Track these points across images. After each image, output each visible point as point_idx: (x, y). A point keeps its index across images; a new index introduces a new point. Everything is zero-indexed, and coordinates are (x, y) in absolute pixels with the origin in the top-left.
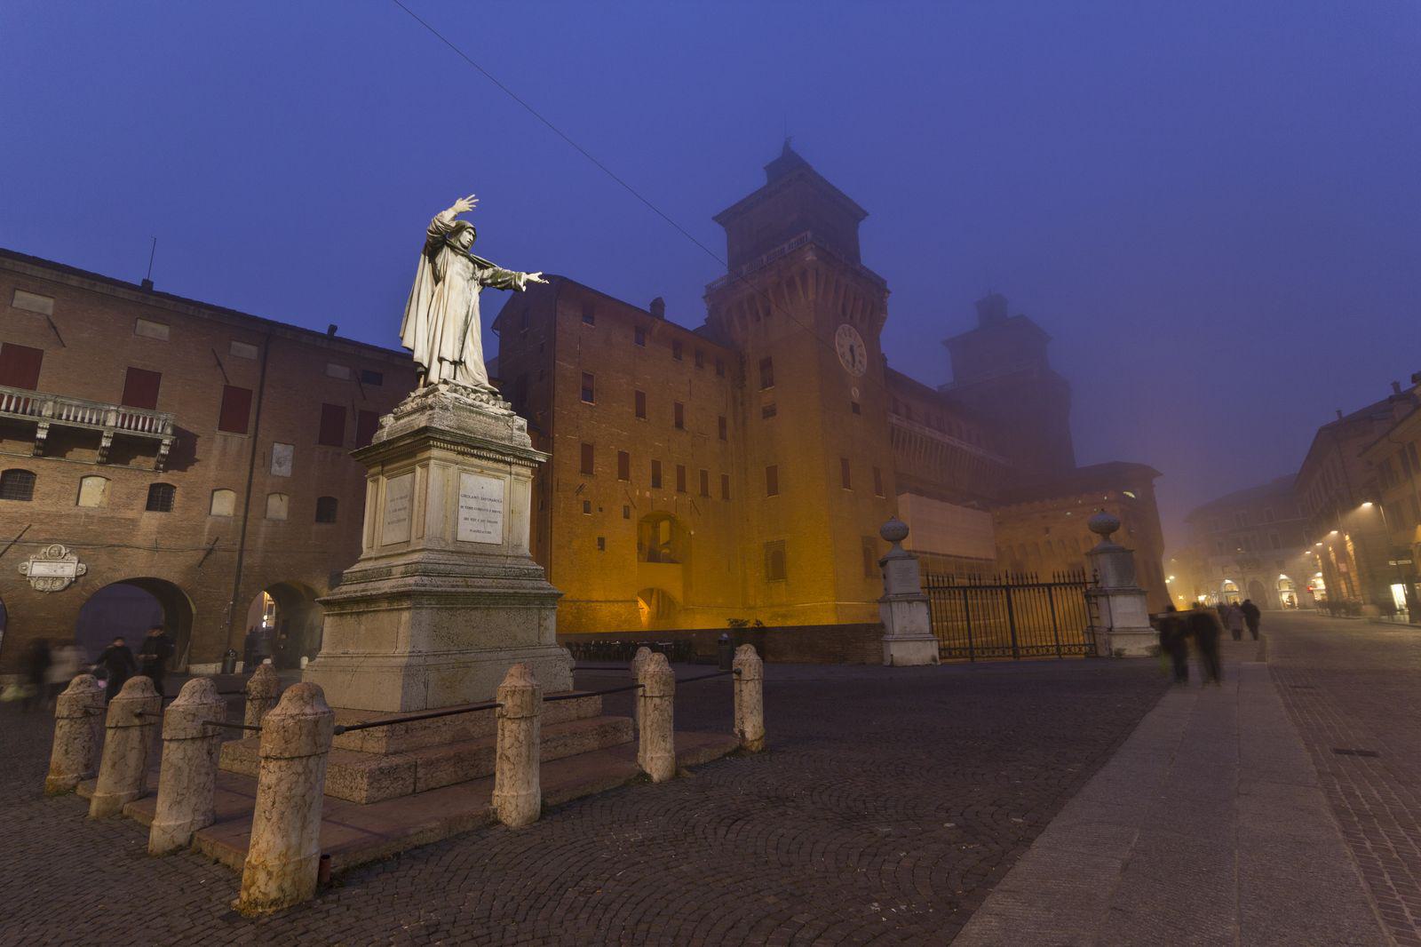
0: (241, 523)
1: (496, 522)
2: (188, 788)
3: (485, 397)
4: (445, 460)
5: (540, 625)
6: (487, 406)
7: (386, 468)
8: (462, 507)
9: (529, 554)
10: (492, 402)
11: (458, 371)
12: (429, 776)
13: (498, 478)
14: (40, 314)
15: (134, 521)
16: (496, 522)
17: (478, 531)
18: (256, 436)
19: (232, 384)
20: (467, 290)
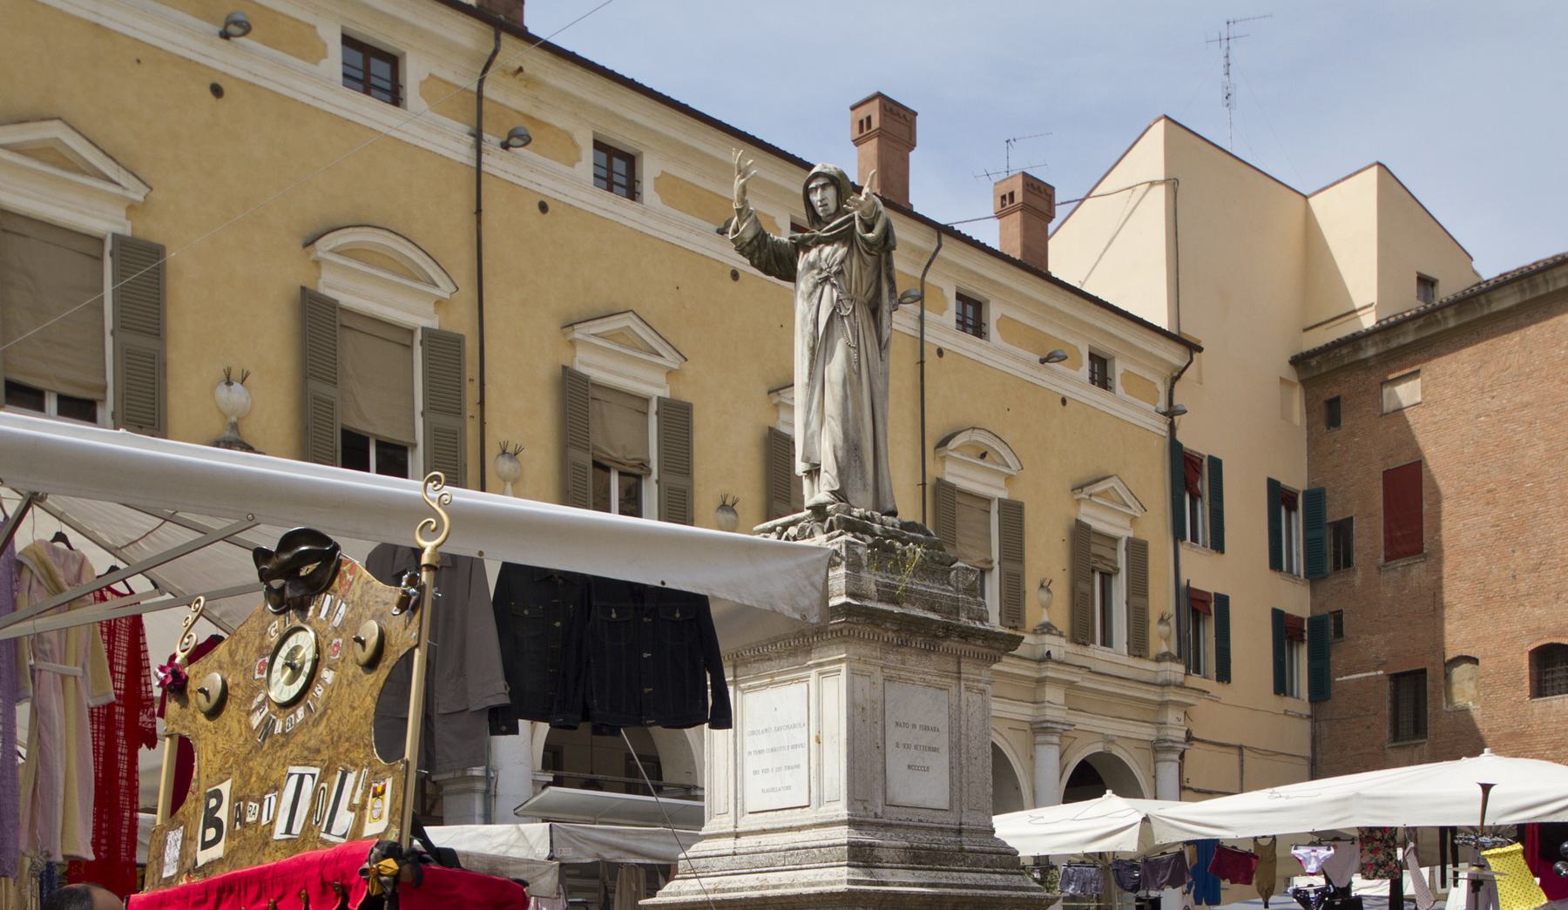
17: (773, 790)
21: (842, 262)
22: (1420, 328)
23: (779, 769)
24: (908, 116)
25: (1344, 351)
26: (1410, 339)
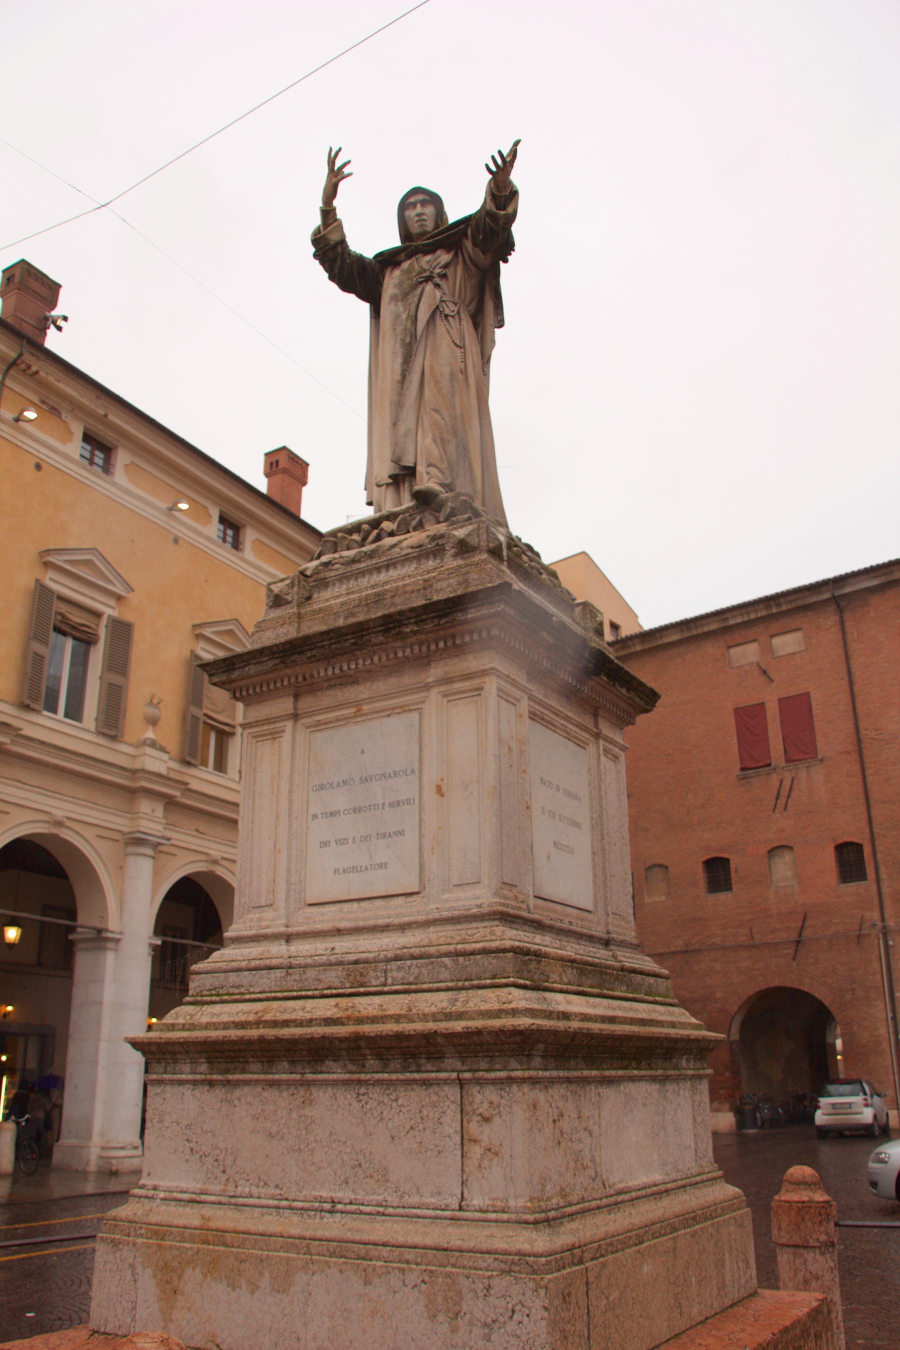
5: (465, 1140)
8: (315, 816)
13: (404, 709)
16: (401, 833)
17: (354, 869)
21: (446, 266)
23: (366, 838)
24: (304, 465)
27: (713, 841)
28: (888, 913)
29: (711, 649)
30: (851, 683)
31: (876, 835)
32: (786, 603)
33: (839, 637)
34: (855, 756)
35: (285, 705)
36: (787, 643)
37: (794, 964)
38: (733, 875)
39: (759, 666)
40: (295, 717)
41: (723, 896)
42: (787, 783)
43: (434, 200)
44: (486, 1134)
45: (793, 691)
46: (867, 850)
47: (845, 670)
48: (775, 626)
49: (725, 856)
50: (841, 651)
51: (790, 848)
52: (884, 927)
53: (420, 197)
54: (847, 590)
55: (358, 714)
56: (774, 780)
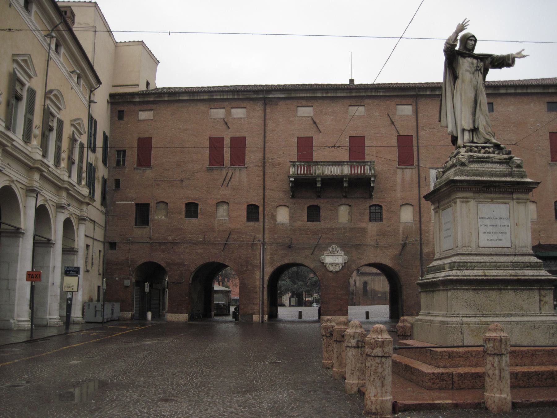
0: (418, 225)
1: (506, 233)
2: (355, 368)
3: (491, 150)
4: (466, 198)
5: (540, 301)
6: (491, 155)
7: (441, 203)
9: (531, 252)
10: (496, 152)
11: (474, 136)
12: (460, 382)
13: (505, 203)
14: (308, 117)
15: (364, 230)
16: (506, 233)
18: (419, 166)
19: (401, 134)
20: (474, 79)
22: (156, 97)
23: (496, 233)
25: (128, 97)
26: (152, 99)
27: (191, 195)
28: (266, 235)
29: (202, 107)
30: (265, 137)
31: (266, 204)
32: (242, 95)
33: (263, 115)
34: (262, 168)
35: (470, 195)
36: (238, 113)
37: (223, 253)
38: (199, 211)
39: (224, 120)
40: (474, 199)
41: (193, 220)
42: (230, 175)
43: (475, 41)
44: (544, 299)
45: (238, 135)
46: (261, 209)
47: (263, 130)
48: (235, 104)
49: (197, 202)
50: (262, 122)
51: (228, 203)
52: (264, 241)
53: (474, 39)
54: (270, 96)
55: (492, 201)
56: (224, 172)
